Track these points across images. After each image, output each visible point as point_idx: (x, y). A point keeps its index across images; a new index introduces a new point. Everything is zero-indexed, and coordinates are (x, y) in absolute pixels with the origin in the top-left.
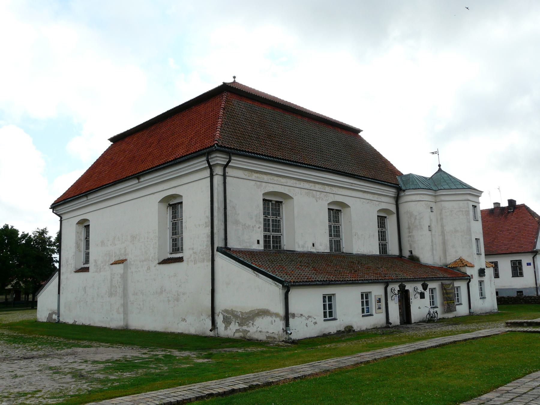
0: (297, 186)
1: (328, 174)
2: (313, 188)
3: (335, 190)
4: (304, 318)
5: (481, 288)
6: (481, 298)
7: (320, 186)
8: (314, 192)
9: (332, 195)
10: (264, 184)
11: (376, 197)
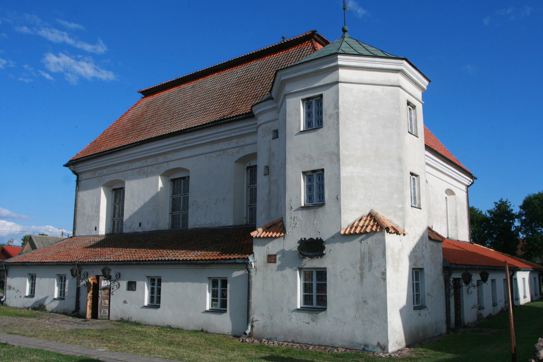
0: (130, 168)
1: (146, 145)
2: (145, 164)
3: (170, 157)
4: (15, 291)
5: (417, 285)
6: (415, 308)
7: (152, 160)
8: (146, 169)
9: (165, 164)
10: (103, 177)
11: (234, 143)
